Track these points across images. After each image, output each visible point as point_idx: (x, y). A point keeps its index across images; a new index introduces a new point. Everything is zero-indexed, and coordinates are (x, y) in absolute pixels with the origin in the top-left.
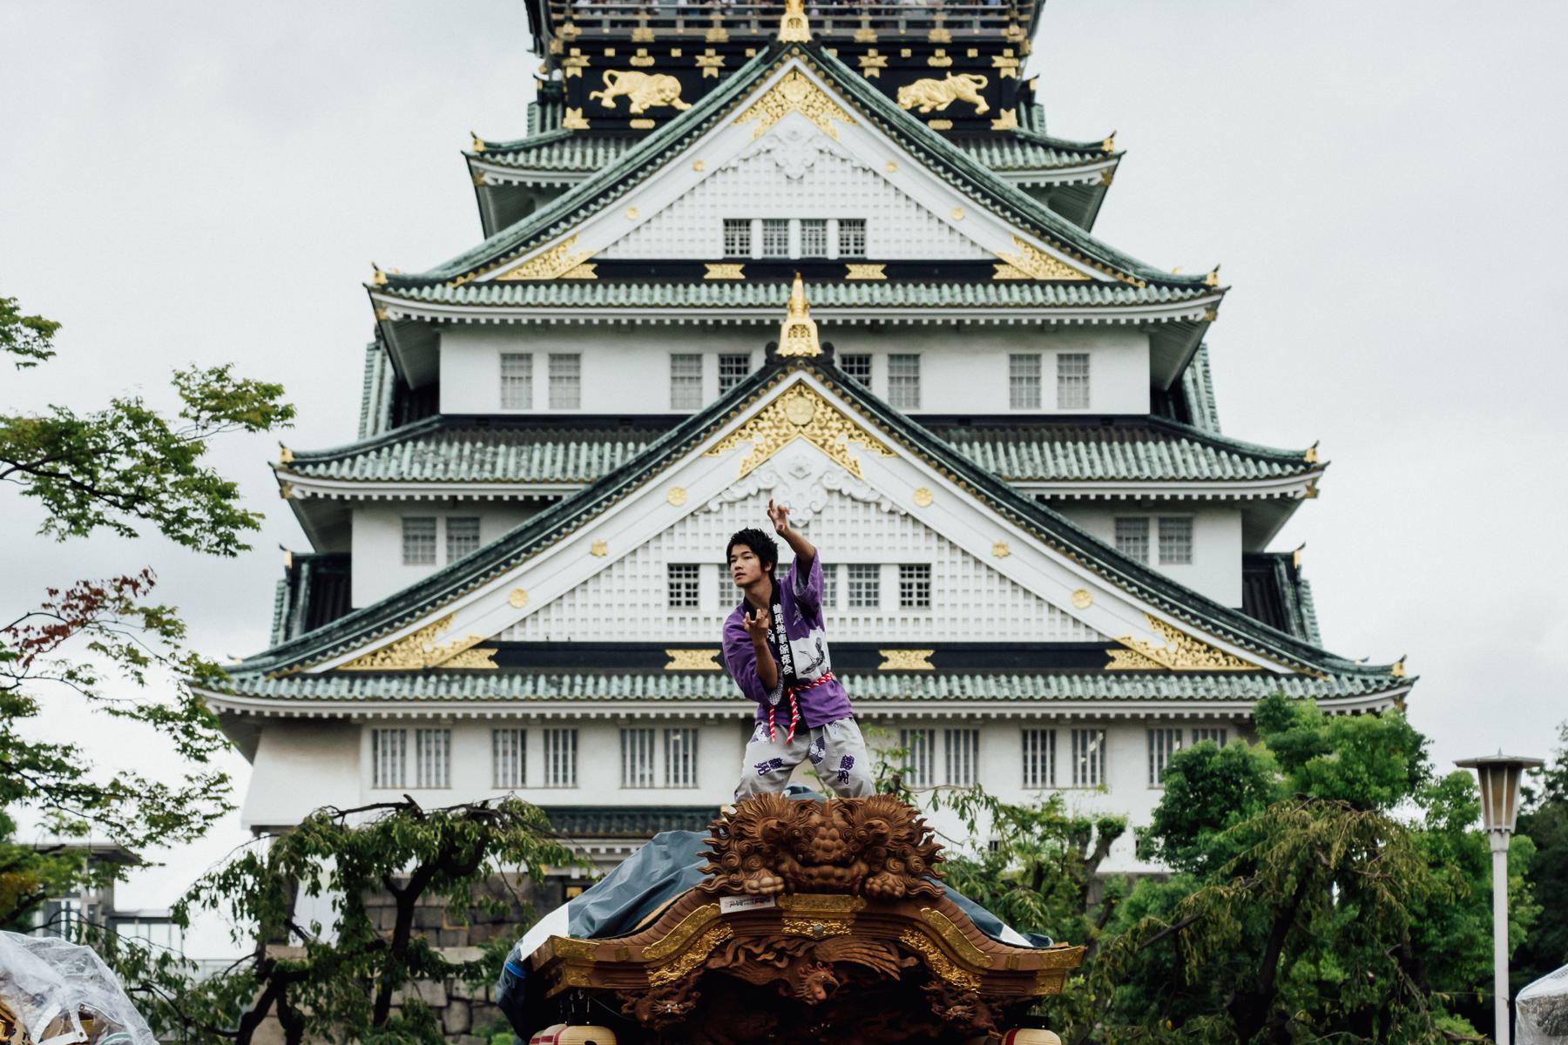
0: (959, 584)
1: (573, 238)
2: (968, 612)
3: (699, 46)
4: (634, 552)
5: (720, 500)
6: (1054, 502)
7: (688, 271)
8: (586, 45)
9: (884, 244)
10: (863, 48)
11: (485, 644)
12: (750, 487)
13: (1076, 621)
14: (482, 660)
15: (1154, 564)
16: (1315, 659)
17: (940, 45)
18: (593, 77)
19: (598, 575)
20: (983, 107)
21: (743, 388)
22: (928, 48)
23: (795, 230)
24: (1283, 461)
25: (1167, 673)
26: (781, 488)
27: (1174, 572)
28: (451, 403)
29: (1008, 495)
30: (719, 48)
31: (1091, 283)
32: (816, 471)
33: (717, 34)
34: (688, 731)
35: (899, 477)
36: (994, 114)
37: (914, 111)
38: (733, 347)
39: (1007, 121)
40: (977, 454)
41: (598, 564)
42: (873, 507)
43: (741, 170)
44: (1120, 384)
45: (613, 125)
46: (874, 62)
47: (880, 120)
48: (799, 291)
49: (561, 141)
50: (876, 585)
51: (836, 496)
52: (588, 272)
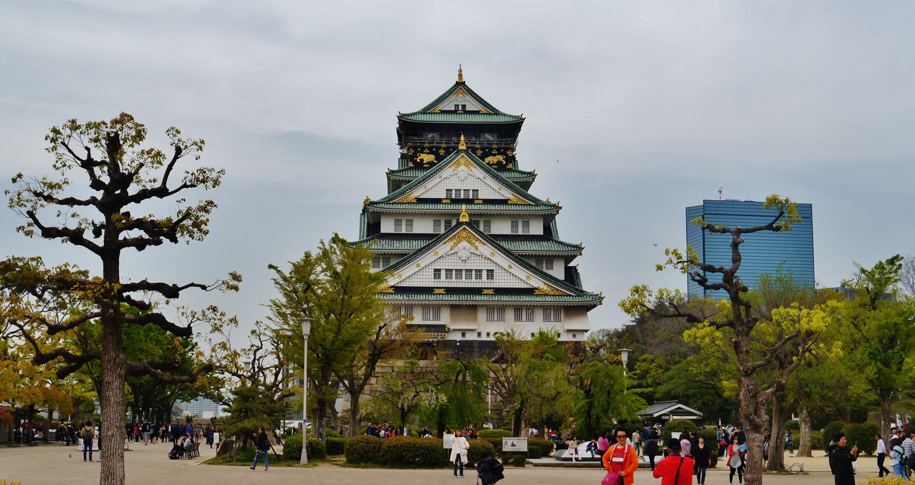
2: (502, 281)
3: (440, 148)
7: (438, 201)
8: (414, 148)
9: (484, 194)
10: (477, 149)
11: (392, 287)
14: (391, 291)
16: (581, 293)
18: (415, 155)
21: (450, 230)
22: (491, 149)
23: (462, 192)
24: (574, 246)
27: (549, 272)
28: (384, 230)
29: (511, 254)
30: (444, 149)
31: (530, 205)
33: (444, 145)
34: (437, 308)
35: (486, 249)
36: (507, 164)
37: (488, 164)
38: (448, 218)
39: (510, 166)
40: (505, 244)
41: (418, 269)
44: (537, 229)
45: (420, 166)
46: (479, 152)
47: (482, 167)
48: (464, 207)
49: (407, 170)
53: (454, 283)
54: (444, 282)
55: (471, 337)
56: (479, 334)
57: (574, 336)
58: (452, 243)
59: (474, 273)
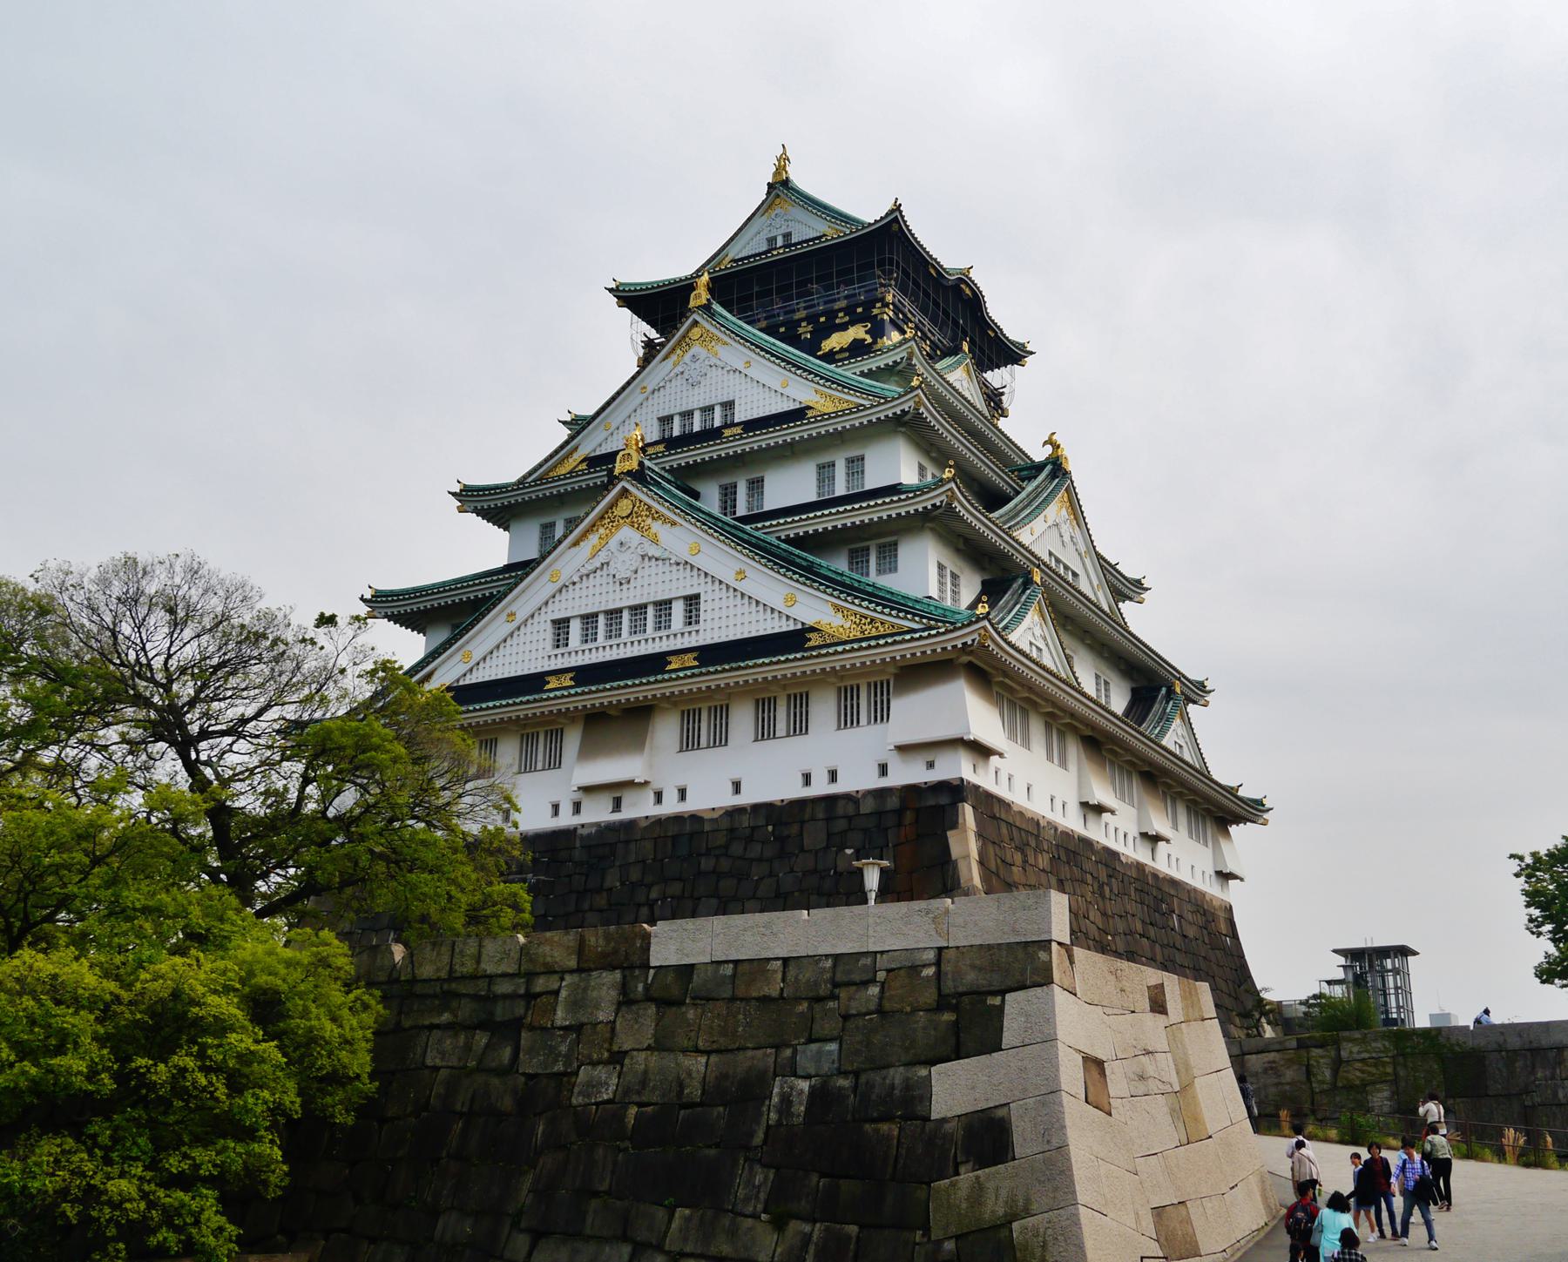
0: (717, 604)
1: (576, 449)
6: (788, 540)
13: (788, 617)
15: (873, 577)
17: (840, 310)
19: (511, 635)
20: (869, 340)
25: (845, 643)
32: (634, 544)
36: (875, 342)
46: (805, 330)
52: (584, 466)
53: (605, 651)
54: (580, 654)
55: (639, 808)
56: (659, 797)
57: (931, 765)
58: (593, 539)
59: (651, 611)
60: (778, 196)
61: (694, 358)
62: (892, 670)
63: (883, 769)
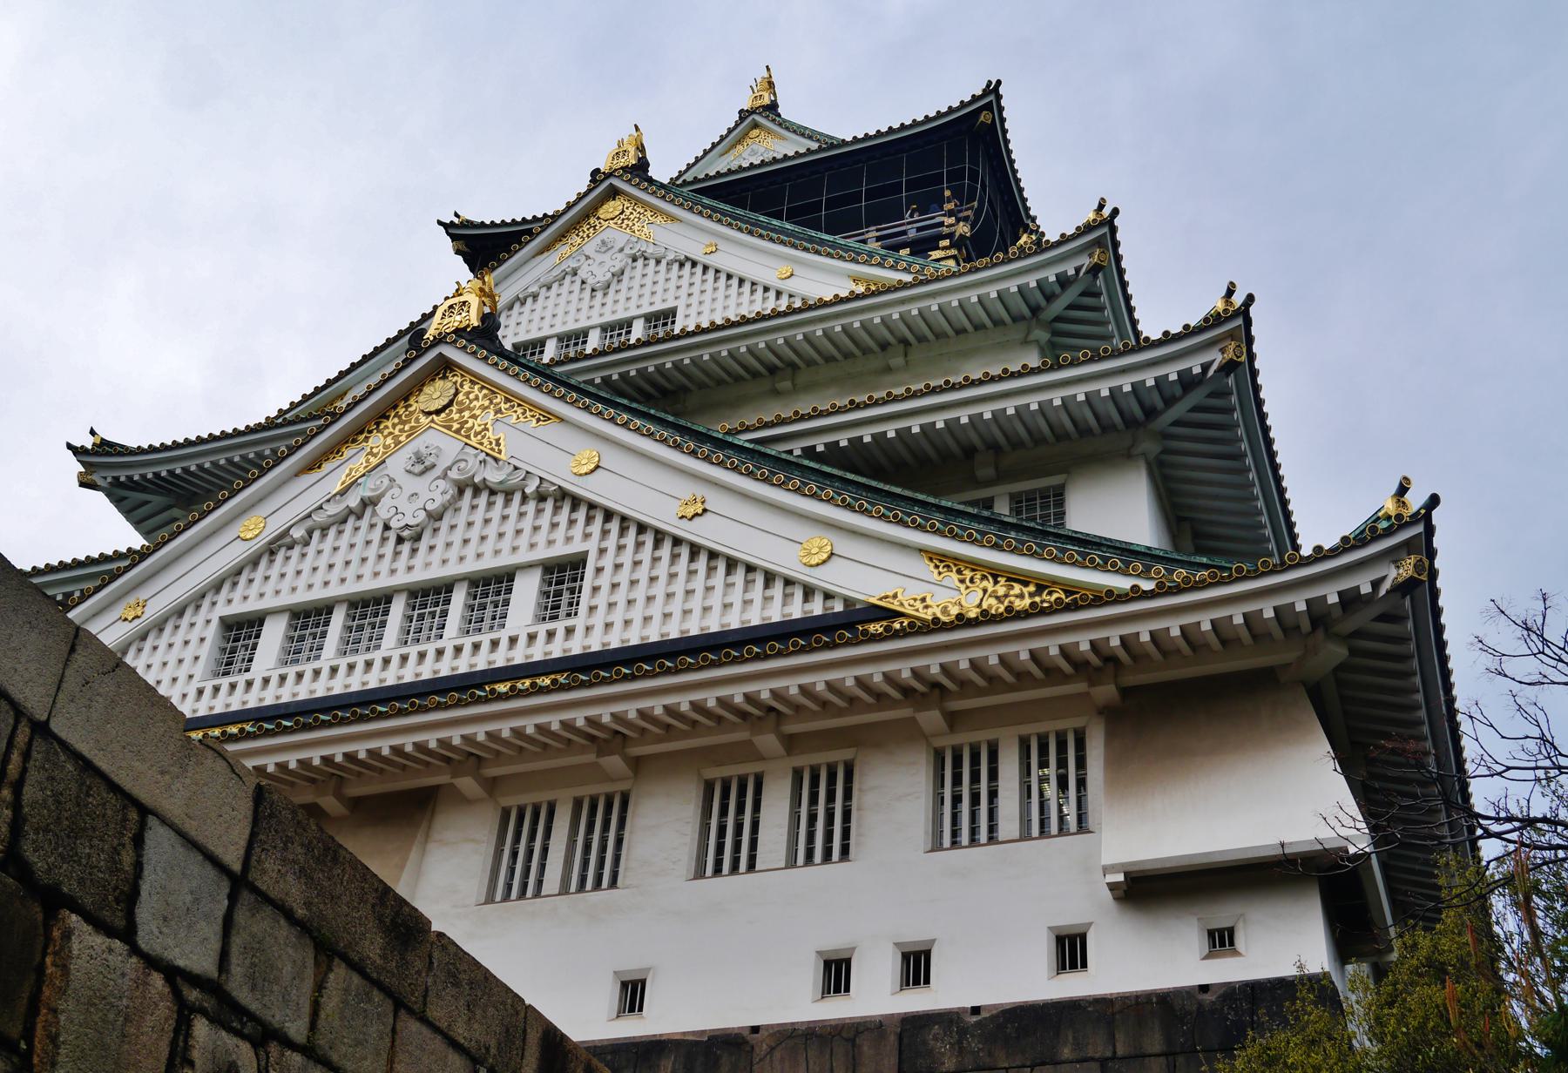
4: (180, 612)
5: (309, 523)
12: (353, 501)
13: (809, 592)
26: (395, 491)
42: (517, 497)
43: (541, 298)
50: (507, 603)
51: (468, 493)
57: (1221, 941)
60: (756, 125)
61: (605, 246)
62: (1106, 692)
63: (1070, 950)
